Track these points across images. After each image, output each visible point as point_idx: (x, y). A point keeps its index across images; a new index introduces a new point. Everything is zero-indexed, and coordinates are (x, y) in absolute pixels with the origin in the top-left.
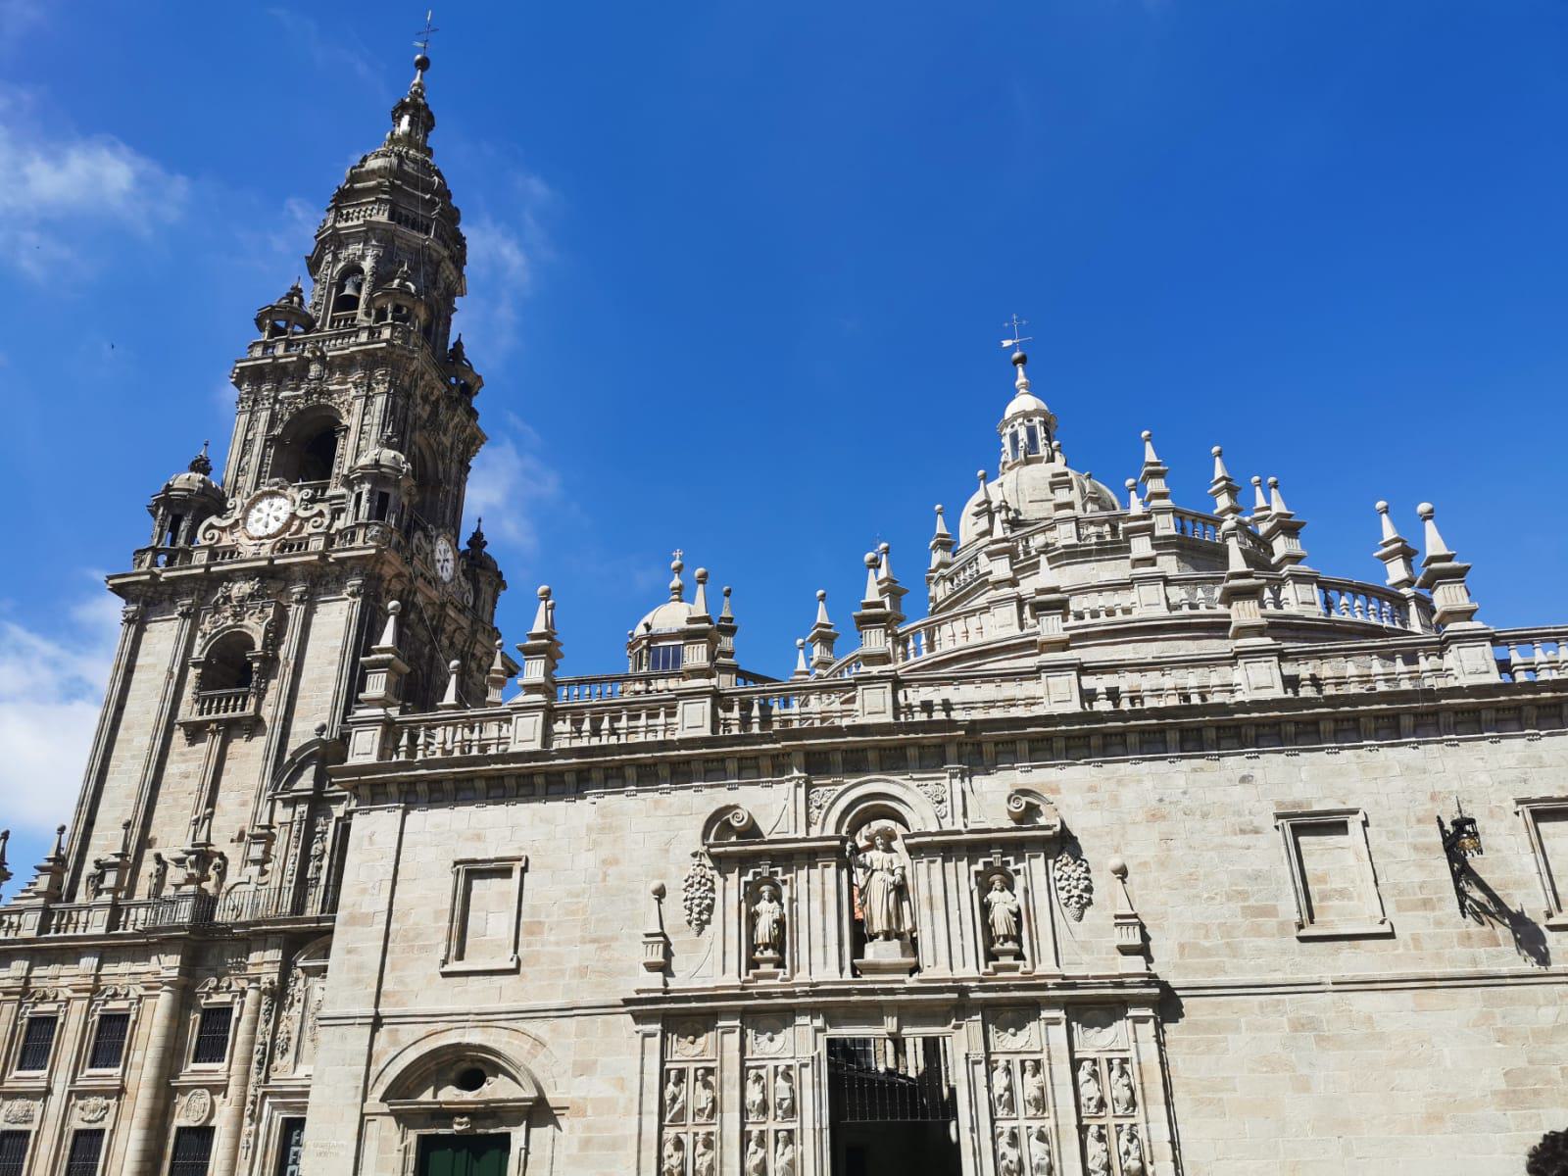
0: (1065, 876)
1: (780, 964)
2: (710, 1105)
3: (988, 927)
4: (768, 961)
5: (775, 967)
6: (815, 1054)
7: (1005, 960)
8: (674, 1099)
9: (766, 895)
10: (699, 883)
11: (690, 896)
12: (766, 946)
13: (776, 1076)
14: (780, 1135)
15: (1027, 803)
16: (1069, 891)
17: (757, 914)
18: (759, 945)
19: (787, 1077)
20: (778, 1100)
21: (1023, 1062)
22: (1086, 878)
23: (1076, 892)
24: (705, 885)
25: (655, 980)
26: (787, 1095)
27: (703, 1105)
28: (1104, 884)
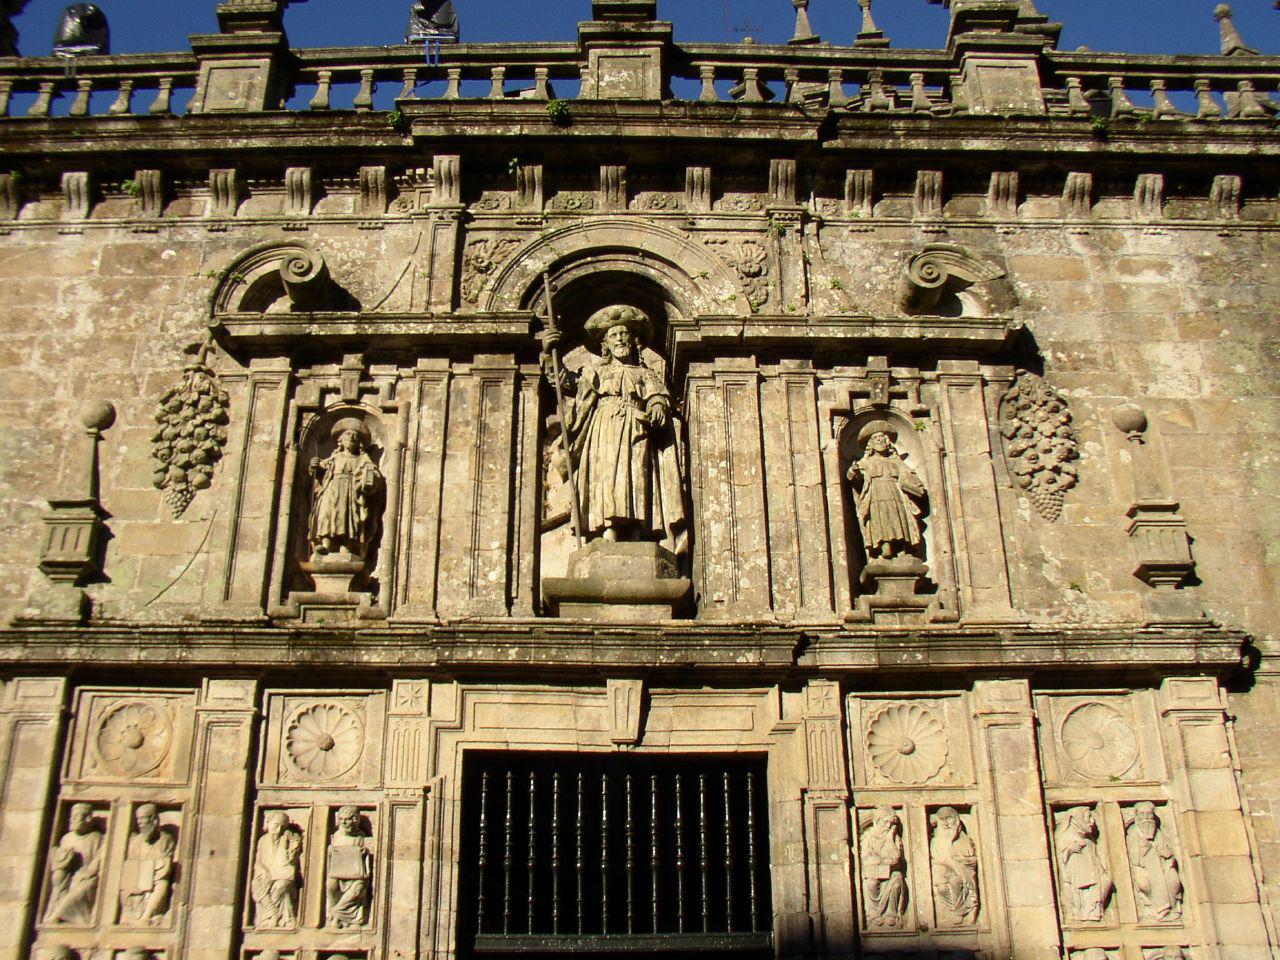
0: (1026, 429)
1: (363, 581)
5: (355, 586)
6: (433, 782)
7: (889, 592)
8: (76, 863)
9: (345, 440)
10: (195, 404)
12: (337, 542)
13: (332, 828)
17: (320, 473)
19: (361, 828)
20: (330, 883)
21: (931, 809)
22: (1068, 436)
23: (1050, 461)
25: (63, 601)
26: (355, 868)
27: (145, 885)
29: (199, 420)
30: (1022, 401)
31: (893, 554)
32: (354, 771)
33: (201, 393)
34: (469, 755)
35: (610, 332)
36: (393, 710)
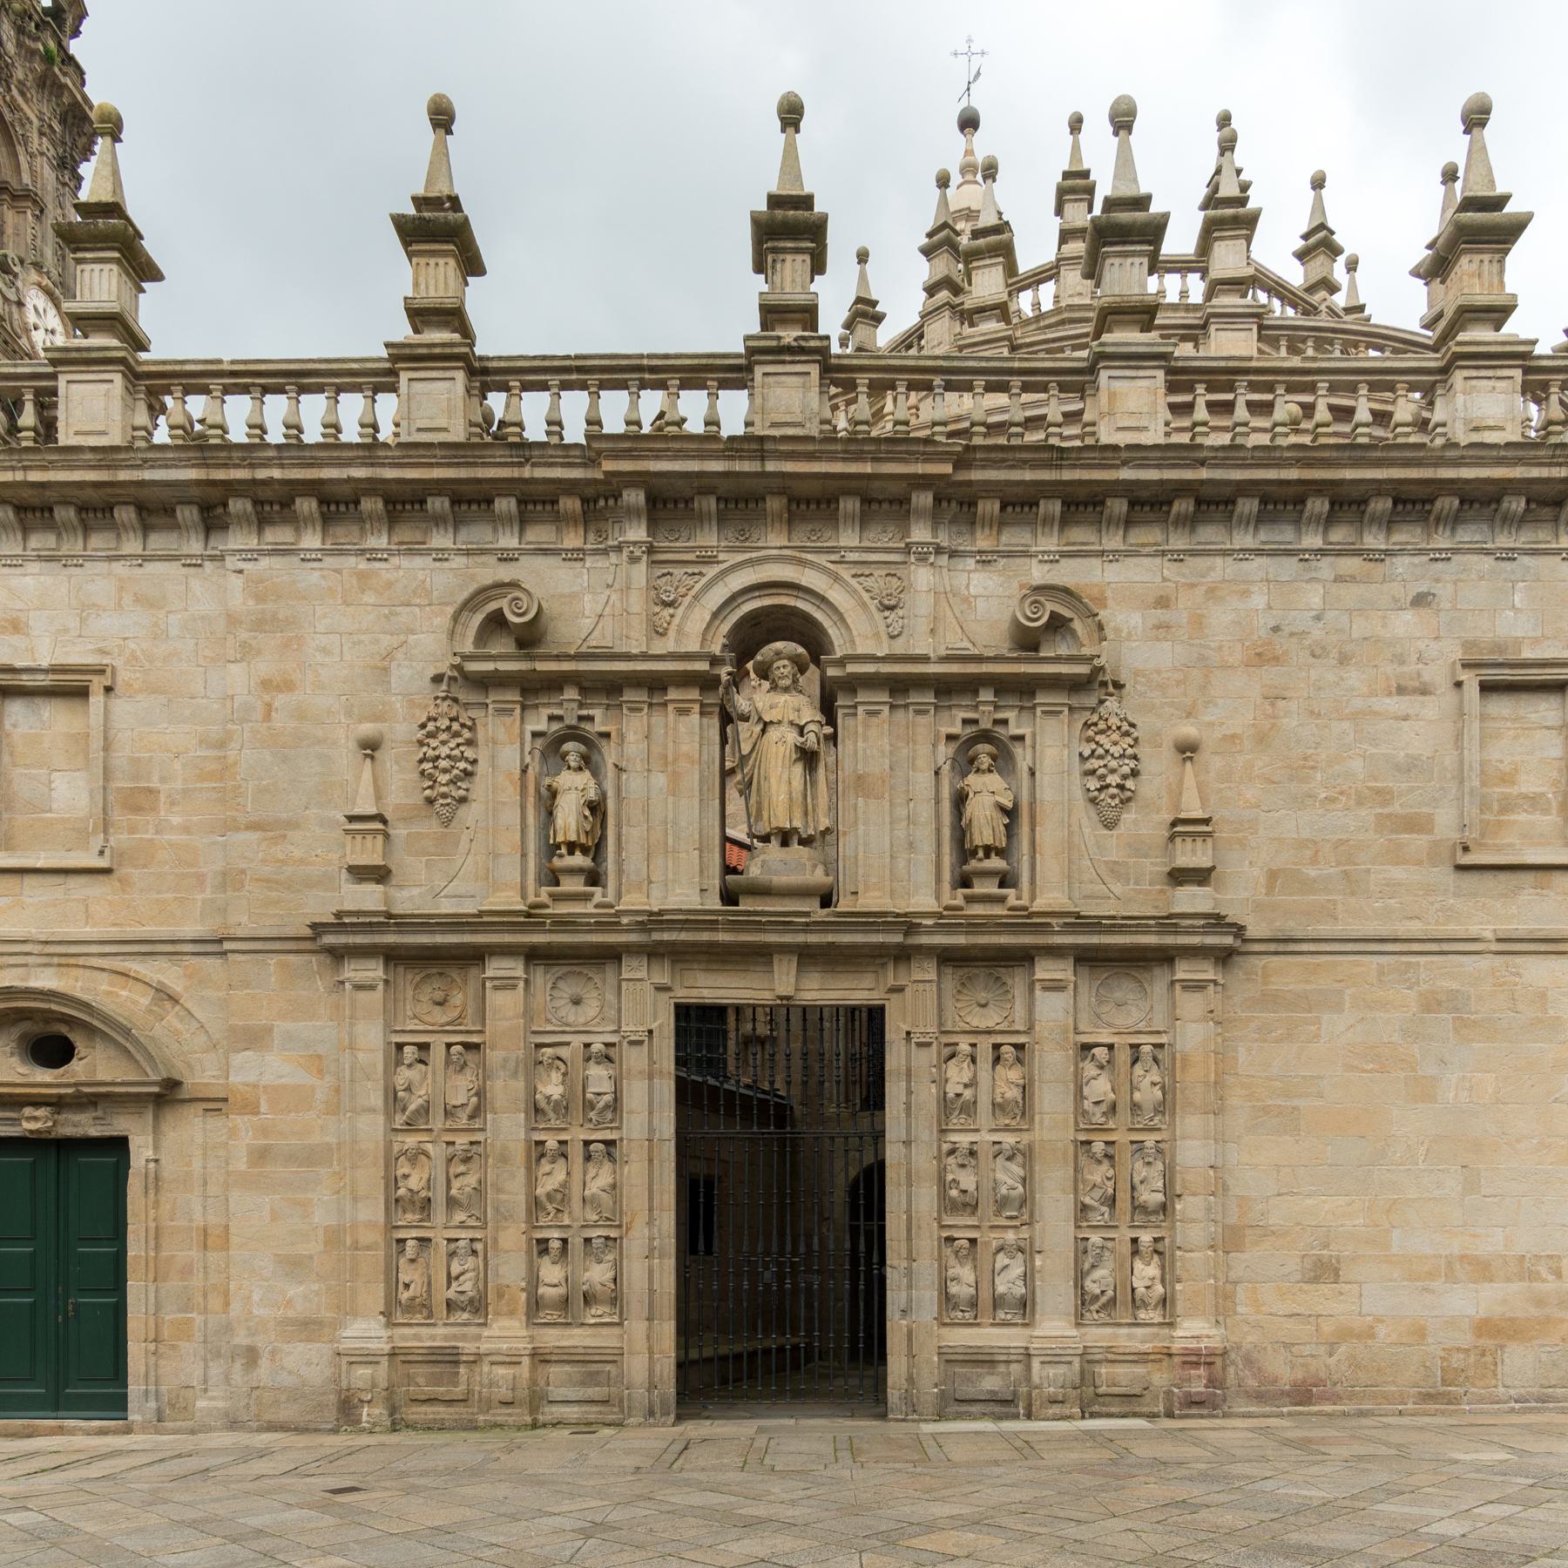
0: (1100, 751)
1: (594, 878)
2: (474, 1100)
3: (961, 833)
4: (572, 871)
9: (573, 760)
10: (449, 728)
11: (431, 753)
12: (572, 847)
14: (592, 1147)
15: (1053, 615)
16: (1103, 777)
17: (554, 794)
18: (558, 847)
21: (996, 1047)
23: (1113, 779)
24: (457, 735)
28: (1158, 766)
29: (452, 745)
30: (1102, 725)
31: (987, 856)
33: (451, 720)
34: (678, 1006)
35: (775, 666)
36: (624, 976)
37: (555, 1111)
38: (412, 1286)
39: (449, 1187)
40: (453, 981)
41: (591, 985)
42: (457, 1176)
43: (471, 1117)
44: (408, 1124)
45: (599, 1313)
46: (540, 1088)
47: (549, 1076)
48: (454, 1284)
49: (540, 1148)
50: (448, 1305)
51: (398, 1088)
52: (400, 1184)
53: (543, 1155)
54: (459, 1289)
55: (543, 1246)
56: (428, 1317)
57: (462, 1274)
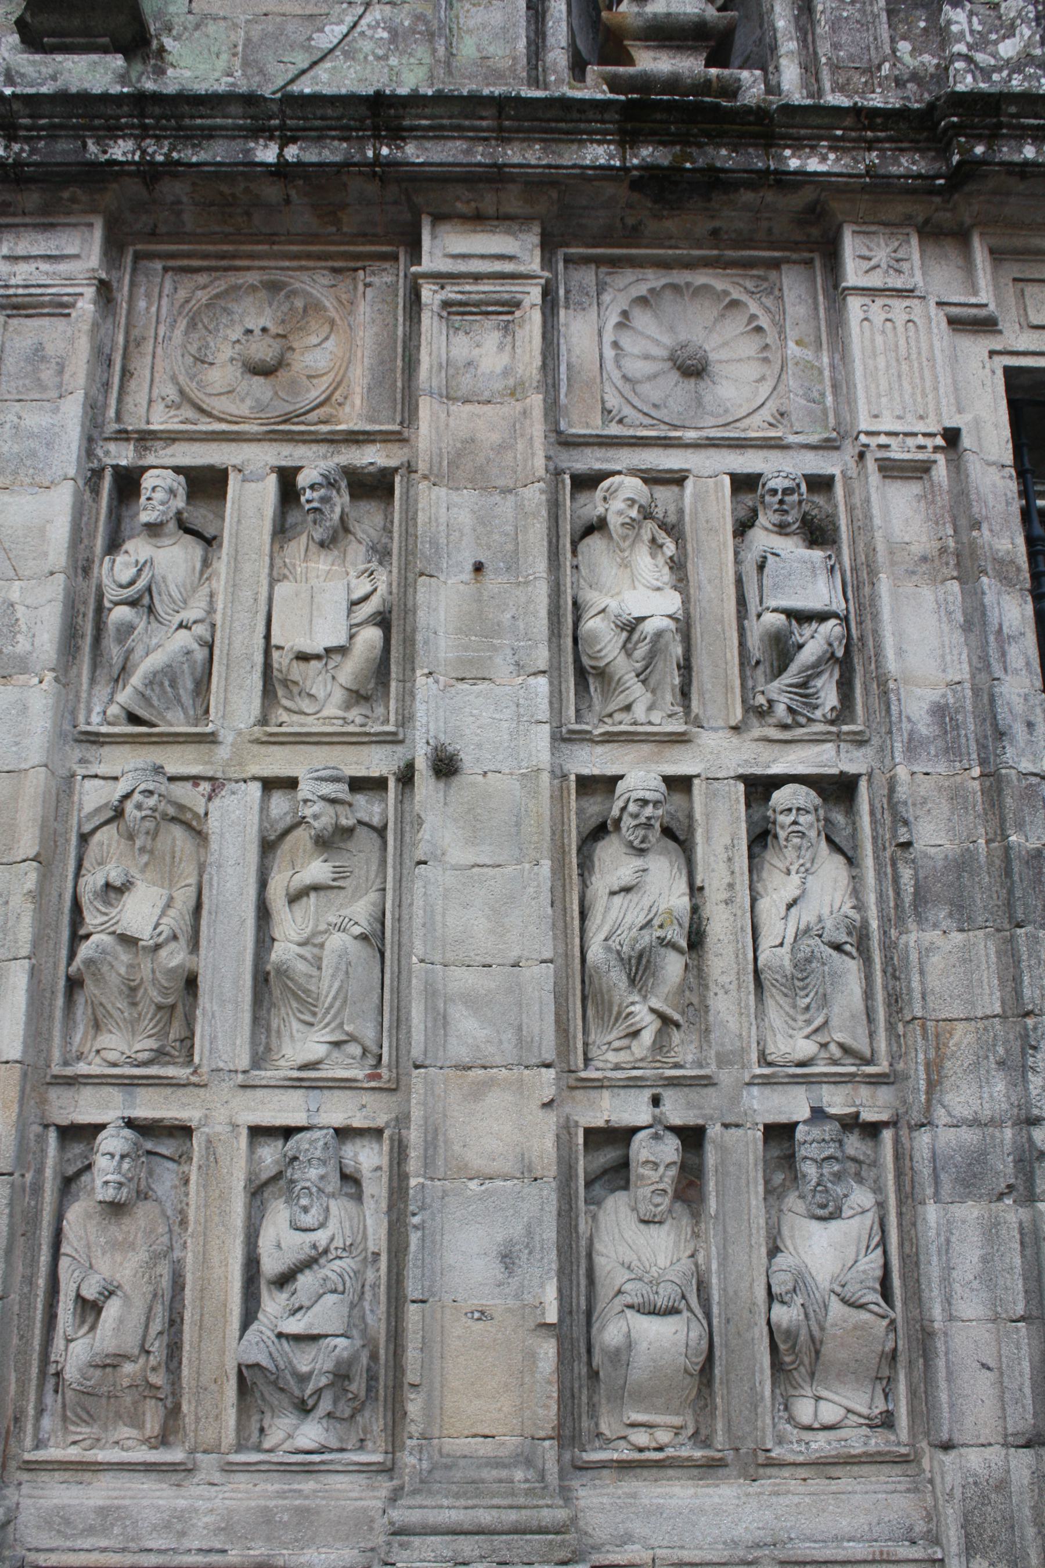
14: (781, 797)
32: (766, 414)
37: (643, 676)
38: (112, 1310)
39: (264, 939)
40: (313, 307)
41: (735, 325)
42: (295, 898)
43: (357, 697)
44: (133, 719)
45: (829, 1413)
46: (594, 599)
47: (625, 564)
48: (272, 1304)
49: (594, 807)
50: (244, 1387)
51: (112, 593)
52: (92, 919)
53: (600, 831)
54: (294, 1326)
55: (607, 1156)
56: (163, 1440)
57: (309, 1263)
